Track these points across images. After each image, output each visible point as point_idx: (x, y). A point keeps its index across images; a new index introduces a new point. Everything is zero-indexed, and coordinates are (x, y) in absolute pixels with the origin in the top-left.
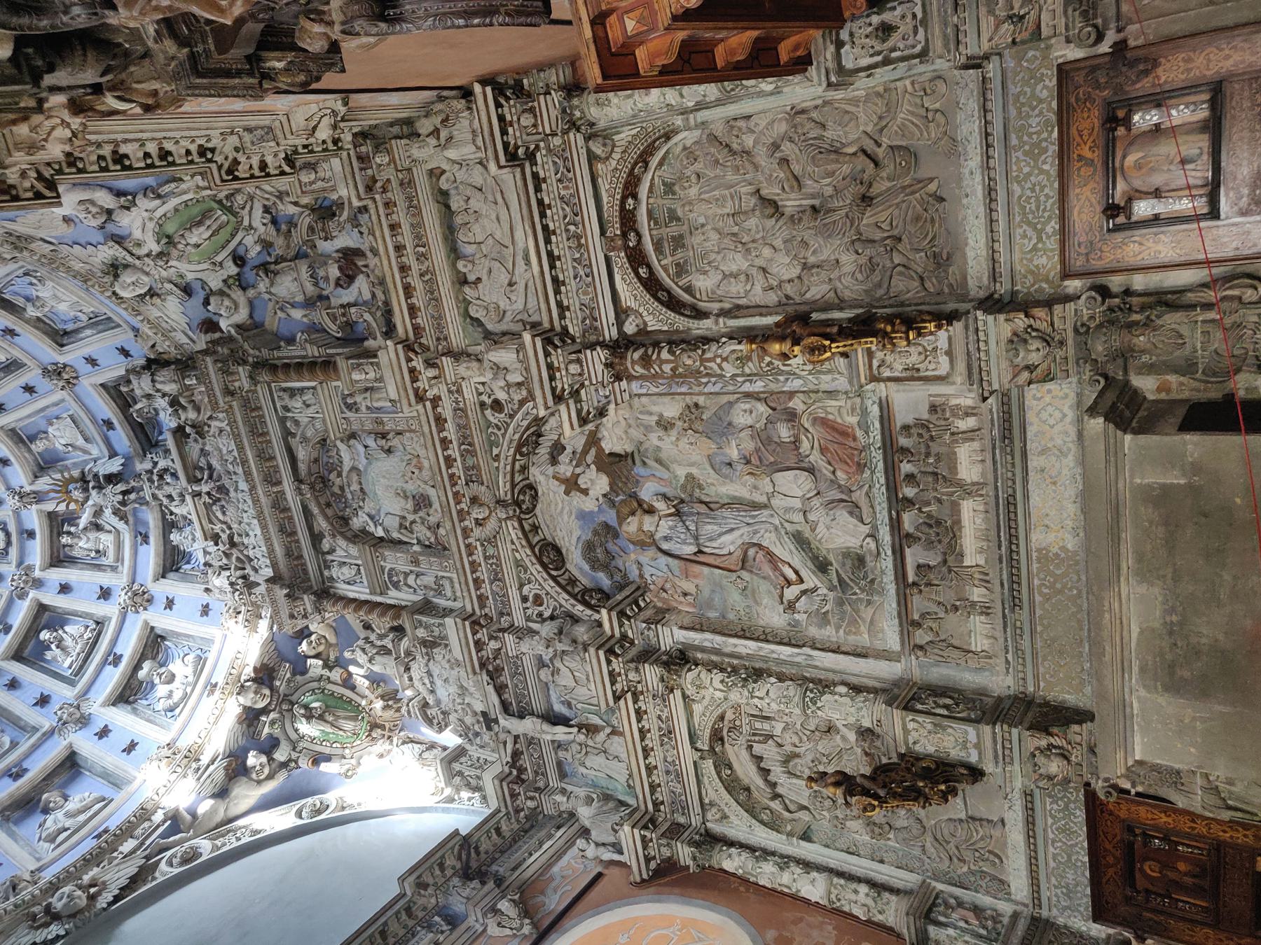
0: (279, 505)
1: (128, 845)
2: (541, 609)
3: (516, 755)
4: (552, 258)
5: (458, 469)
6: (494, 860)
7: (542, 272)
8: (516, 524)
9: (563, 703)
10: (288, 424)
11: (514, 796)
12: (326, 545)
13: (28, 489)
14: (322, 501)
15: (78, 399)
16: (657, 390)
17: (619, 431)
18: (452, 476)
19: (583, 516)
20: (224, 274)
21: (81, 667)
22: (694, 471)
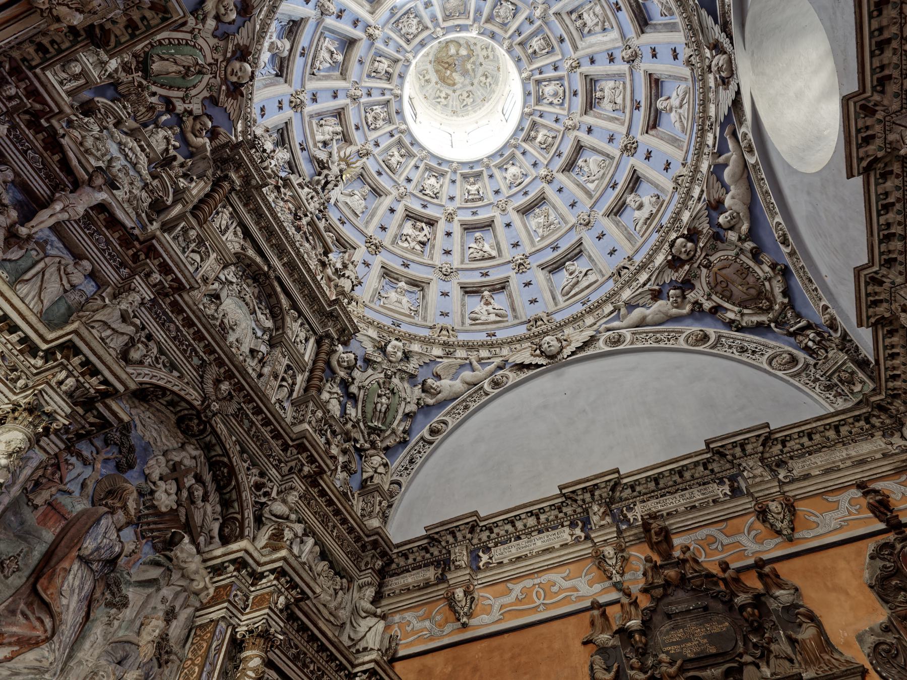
0: (281, 251)
4: (313, 638)
5: (248, 409)
7: (316, 625)
8: (196, 403)
9: (46, 242)
10: (297, 315)
11: (32, 93)
13: (365, 159)
14: (254, 268)
15: (362, 232)
16: (214, 646)
17: (193, 567)
18: (252, 400)
19: (147, 449)
20: (356, 383)
21: (319, 40)
22: (128, 613)
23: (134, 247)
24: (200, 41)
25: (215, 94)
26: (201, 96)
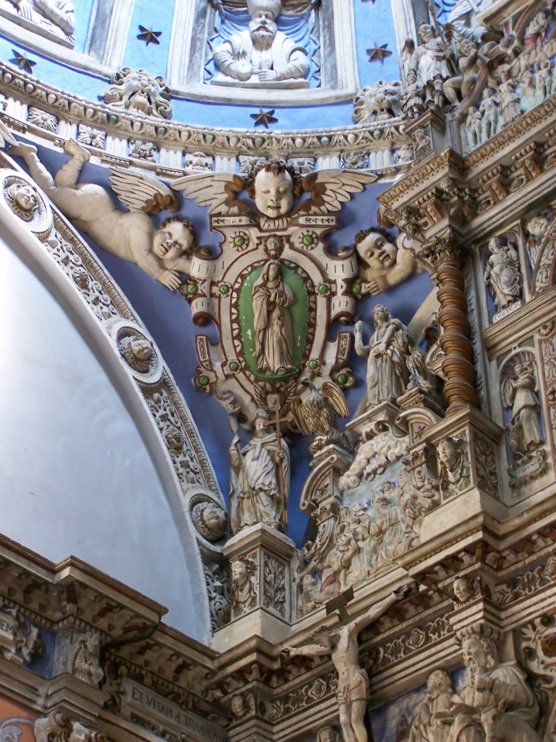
1: (17, 110)
2: (540, 653)
3: (304, 661)
6: (139, 679)
12: (536, 227)
23: (427, 591)
24: (230, 278)
25: (319, 231)
26: (324, 260)
